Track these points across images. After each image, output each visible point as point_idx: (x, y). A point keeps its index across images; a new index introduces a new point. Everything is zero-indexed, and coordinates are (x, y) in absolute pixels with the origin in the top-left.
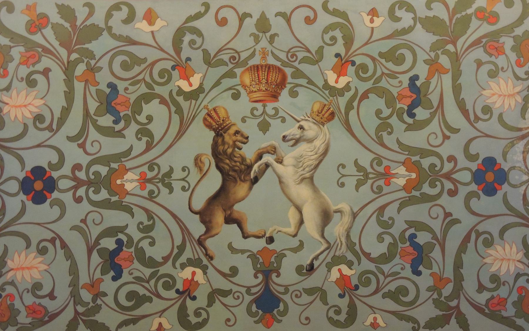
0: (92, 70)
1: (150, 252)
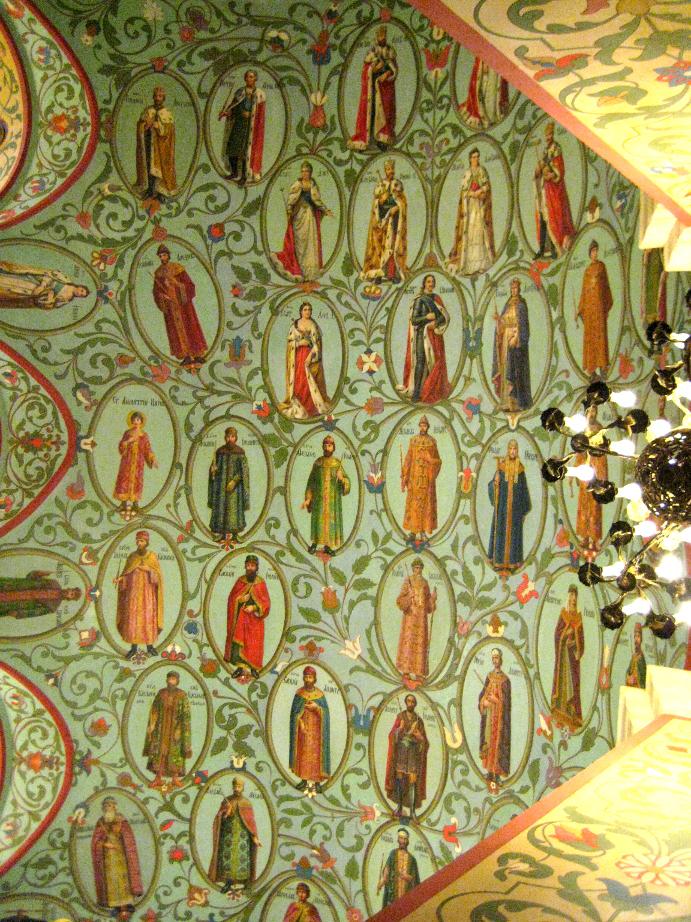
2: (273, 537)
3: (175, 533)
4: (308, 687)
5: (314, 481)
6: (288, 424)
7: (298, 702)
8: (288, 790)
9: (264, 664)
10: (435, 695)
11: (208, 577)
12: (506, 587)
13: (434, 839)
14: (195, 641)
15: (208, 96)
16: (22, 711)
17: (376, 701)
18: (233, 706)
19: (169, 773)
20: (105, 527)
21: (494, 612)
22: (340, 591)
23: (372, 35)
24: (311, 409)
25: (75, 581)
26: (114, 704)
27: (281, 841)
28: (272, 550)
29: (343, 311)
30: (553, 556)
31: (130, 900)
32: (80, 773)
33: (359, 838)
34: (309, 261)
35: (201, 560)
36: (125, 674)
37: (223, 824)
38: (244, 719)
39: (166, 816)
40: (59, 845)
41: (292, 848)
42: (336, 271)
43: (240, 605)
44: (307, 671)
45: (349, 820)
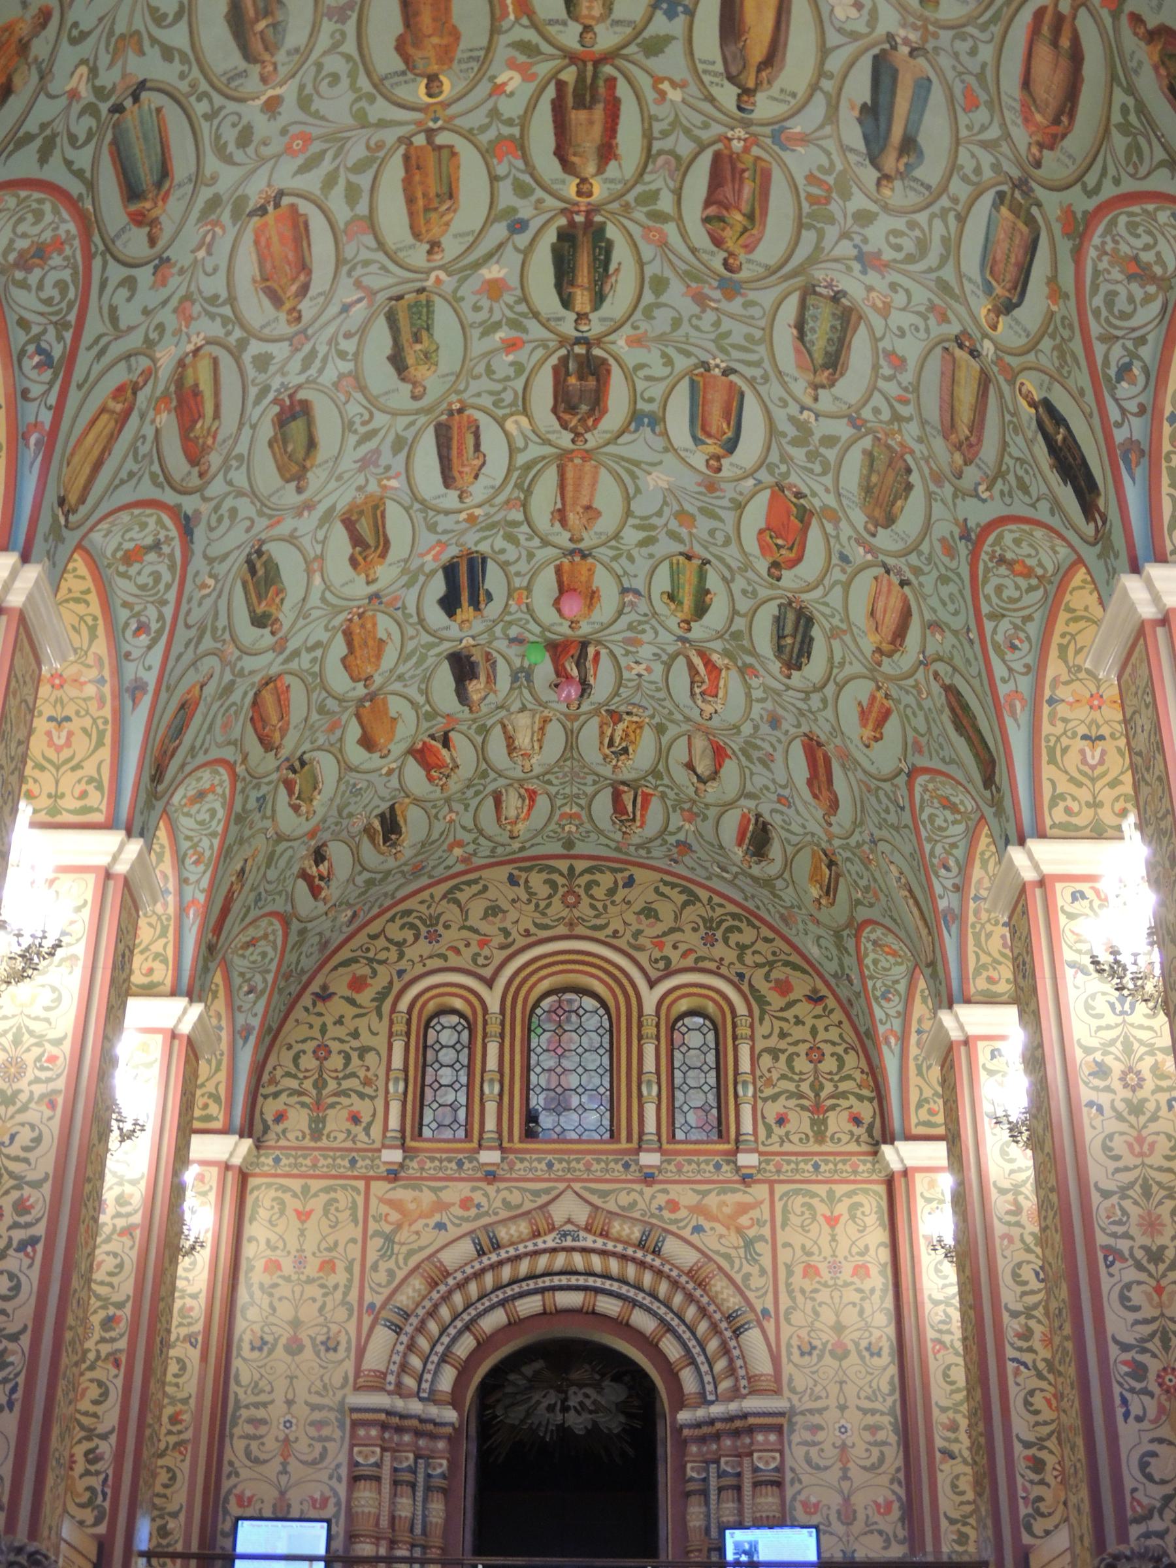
5: (701, 609)
6: (726, 653)
7: (731, 446)
8: (749, 372)
10: (548, 450)
13: (536, 330)
15: (780, 876)
16: (1016, 627)
19: (888, 447)
22: (674, 525)
23: (636, 840)
24: (702, 654)
25: (936, 688)
27: (762, 323)
28: (750, 574)
29: (667, 703)
34: (700, 743)
35: (826, 604)
42: (673, 730)
44: (719, 470)
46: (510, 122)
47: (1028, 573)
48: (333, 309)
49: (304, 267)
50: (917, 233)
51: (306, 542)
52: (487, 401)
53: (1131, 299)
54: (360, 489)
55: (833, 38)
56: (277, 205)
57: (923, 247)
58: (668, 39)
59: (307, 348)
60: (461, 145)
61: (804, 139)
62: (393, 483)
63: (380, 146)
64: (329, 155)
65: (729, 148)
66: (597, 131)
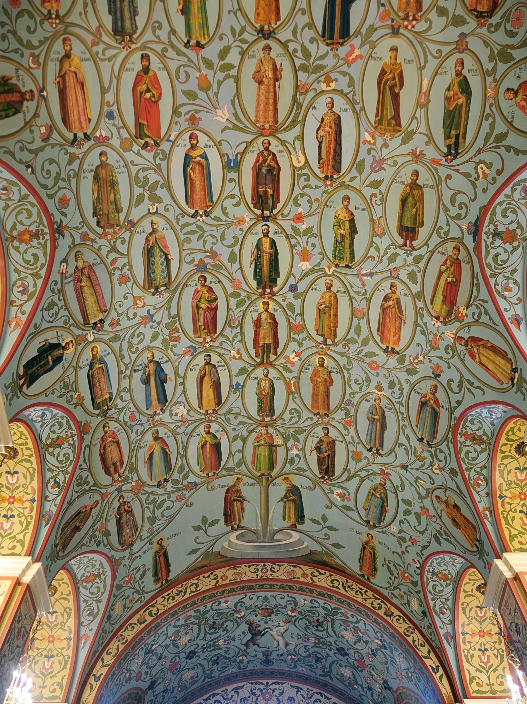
0: (206, 621)
1: (227, 656)
2: (158, 37)
3: (89, 38)
4: (193, 147)
7: (187, 159)
9: (162, 136)
11: (116, 74)
12: (336, 56)
13: (287, 225)
14: (114, 125)
16: (10, 199)
17: (241, 149)
18: (144, 170)
19: (112, 226)
20: (40, 35)
21: (327, 74)
26: (69, 181)
27: (185, 253)
28: (159, 48)
30: (376, 29)
31: (101, 316)
32: (59, 238)
33: (236, 238)
35: (109, 59)
36: (73, 158)
37: (148, 251)
38: (153, 177)
39: (113, 255)
40: (56, 291)
41: (193, 255)
43: (141, 93)
45: (228, 229)
46: (295, 340)
47: (20, 238)
48: (377, 278)
49: (384, 310)
50: (133, 350)
51: (423, 128)
52: (314, 181)
53: (54, 432)
54: (385, 145)
55: (182, 399)
56: (387, 347)
57: (130, 345)
58: (237, 375)
59: (392, 266)
60: (313, 333)
61: (184, 354)
62: (368, 138)
63: (344, 346)
64: (363, 353)
65: (211, 337)
66: (262, 335)
